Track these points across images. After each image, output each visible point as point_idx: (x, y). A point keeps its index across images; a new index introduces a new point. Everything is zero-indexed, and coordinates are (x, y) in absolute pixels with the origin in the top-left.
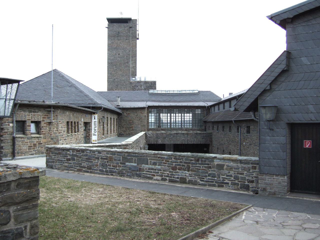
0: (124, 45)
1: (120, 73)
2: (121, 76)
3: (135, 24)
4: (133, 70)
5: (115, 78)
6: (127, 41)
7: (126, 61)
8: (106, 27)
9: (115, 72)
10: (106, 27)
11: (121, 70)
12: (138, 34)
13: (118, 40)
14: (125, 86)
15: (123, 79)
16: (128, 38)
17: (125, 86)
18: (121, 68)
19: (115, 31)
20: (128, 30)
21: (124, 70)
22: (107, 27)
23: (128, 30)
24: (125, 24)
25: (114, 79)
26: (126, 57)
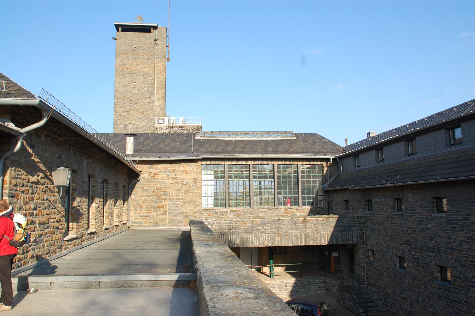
0: (143, 69)
1: (137, 115)
2: (138, 120)
4: (159, 111)
5: (127, 123)
6: (149, 62)
7: (148, 96)
12: (169, 51)
13: (135, 60)
15: (141, 125)
16: (151, 57)
18: (138, 107)
19: (129, 45)
20: (151, 44)
21: (144, 110)
23: (151, 44)
24: (146, 34)
25: (127, 125)
26: (146, 88)
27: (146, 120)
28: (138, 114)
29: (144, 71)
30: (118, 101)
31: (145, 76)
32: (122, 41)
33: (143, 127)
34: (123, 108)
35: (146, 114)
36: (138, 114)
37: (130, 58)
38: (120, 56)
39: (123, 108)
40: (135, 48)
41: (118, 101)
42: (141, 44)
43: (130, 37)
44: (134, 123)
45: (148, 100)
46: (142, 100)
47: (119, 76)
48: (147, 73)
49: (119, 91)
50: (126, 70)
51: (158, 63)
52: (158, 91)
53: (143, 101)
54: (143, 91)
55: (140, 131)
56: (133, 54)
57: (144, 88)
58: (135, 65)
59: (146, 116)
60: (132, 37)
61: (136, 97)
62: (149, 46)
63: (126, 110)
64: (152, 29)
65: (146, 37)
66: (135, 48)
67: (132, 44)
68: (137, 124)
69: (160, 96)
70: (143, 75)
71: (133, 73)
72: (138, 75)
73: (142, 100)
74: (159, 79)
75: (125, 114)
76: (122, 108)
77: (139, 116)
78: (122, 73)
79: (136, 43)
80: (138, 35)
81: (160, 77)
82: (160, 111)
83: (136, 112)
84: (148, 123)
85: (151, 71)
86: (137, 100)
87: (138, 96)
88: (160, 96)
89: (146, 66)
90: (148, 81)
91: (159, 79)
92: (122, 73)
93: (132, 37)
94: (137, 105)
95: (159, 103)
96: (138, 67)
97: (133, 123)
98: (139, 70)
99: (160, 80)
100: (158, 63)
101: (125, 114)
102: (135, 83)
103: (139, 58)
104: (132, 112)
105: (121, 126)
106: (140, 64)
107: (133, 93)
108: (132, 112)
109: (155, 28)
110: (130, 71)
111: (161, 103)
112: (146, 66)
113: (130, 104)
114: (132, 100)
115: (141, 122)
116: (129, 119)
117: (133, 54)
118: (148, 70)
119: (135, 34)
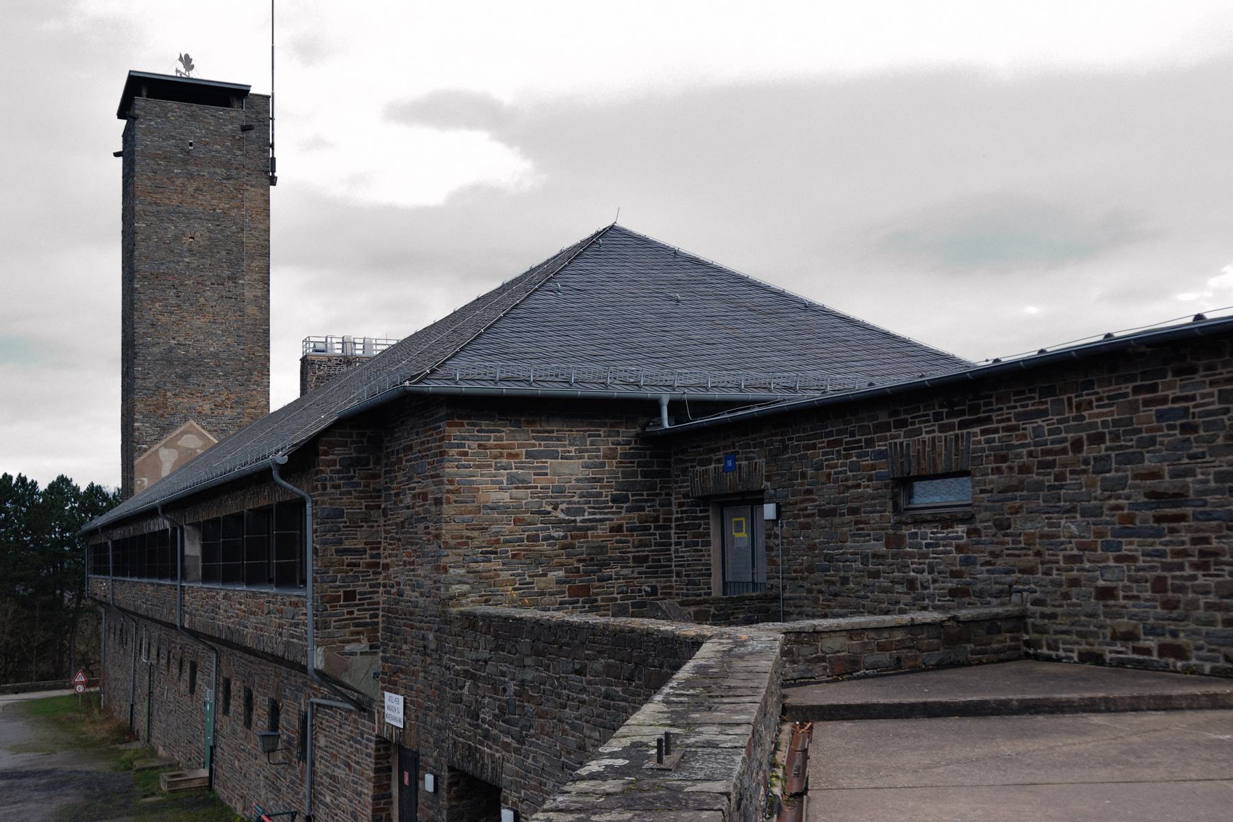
0: (214, 202)
2: (202, 337)
3: (260, 116)
4: (254, 314)
5: (173, 342)
7: (227, 273)
8: (117, 155)
9: (173, 318)
10: (117, 155)
11: (201, 310)
13: (191, 176)
14: (219, 381)
15: (212, 349)
16: (234, 172)
17: (219, 381)
18: (202, 300)
19: (174, 138)
20: (234, 137)
22: (120, 149)
24: (221, 112)
27: (223, 336)
29: (214, 210)
32: (152, 123)
33: (215, 355)
40: (191, 144)
42: (205, 137)
44: (191, 343)
46: (213, 284)
47: (148, 218)
48: (225, 213)
49: (147, 258)
51: (249, 188)
52: (252, 262)
53: (216, 286)
55: (208, 363)
56: (185, 162)
57: (218, 253)
59: (224, 326)
65: (221, 119)
66: (191, 144)
71: (186, 211)
73: (213, 284)
74: (252, 232)
76: (157, 305)
82: (258, 314)
83: (198, 314)
84: (228, 345)
86: (198, 283)
88: (256, 276)
91: (252, 232)
94: (199, 296)
95: (254, 293)
96: (200, 197)
98: (202, 205)
99: (256, 234)
100: (249, 188)
101: (164, 319)
103: (202, 173)
104: (185, 314)
105: (156, 350)
108: (185, 314)
115: (211, 342)
117: (185, 162)
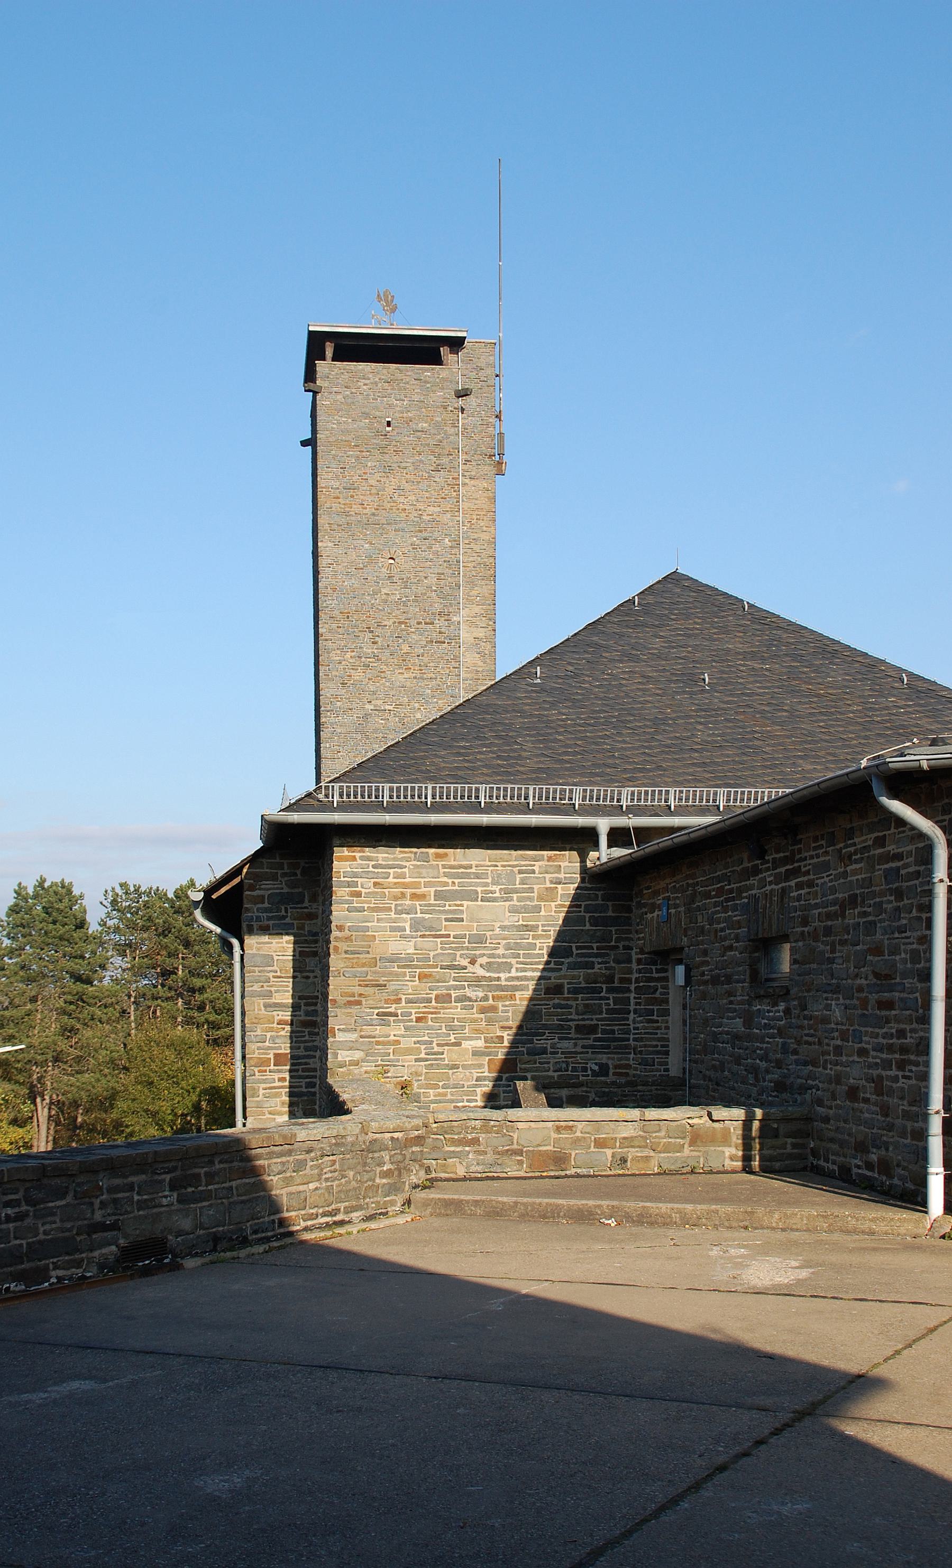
0: (420, 506)
1: (401, 678)
2: (406, 699)
6: (440, 477)
7: (437, 607)
13: (388, 470)
16: (445, 460)
19: (366, 415)
21: (426, 659)
25: (366, 716)
26: (432, 580)
28: (406, 676)
30: (334, 626)
31: (425, 535)
32: (339, 397)
34: (353, 654)
35: (434, 676)
36: (406, 676)
37: (369, 464)
38: (334, 457)
39: (353, 654)
41: (334, 626)
43: (368, 382)
45: (440, 623)
46: (419, 623)
50: (356, 508)
54: (421, 589)
56: (383, 450)
58: (389, 490)
60: (376, 383)
61: (398, 612)
62: (439, 419)
63: (363, 659)
64: (444, 350)
67: (376, 408)
68: (402, 711)
69: (477, 609)
70: (421, 531)
72: (403, 530)
73: (419, 623)
74: (472, 546)
75: (358, 675)
76: (348, 655)
77: (408, 684)
78: (342, 520)
79: (391, 406)
80: (399, 376)
81: (476, 536)
82: (481, 664)
83: (400, 666)
85: (448, 515)
87: (406, 609)
89: (427, 495)
90: (436, 553)
91: (472, 546)
92: (342, 520)
93: (376, 383)
94: (401, 641)
96: (402, 499)
97: (388, 707)
99: (477, 548)
102: (392, 561)
103: (403, 465)
105: (347, 719)
106: (407, 486)
107: (384, 597)
109: (456, 344)
110: (373, 514)
111: (481, 633)
112: (427, 495)
113: (377, 639)
114: (385, 623)
116: (374, 693)
117: (383, 450)
118: (438, 509)
119: (385, 371)
